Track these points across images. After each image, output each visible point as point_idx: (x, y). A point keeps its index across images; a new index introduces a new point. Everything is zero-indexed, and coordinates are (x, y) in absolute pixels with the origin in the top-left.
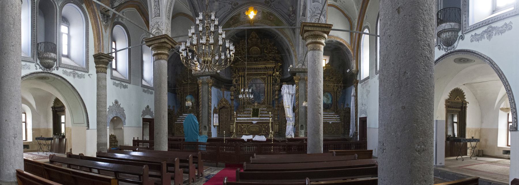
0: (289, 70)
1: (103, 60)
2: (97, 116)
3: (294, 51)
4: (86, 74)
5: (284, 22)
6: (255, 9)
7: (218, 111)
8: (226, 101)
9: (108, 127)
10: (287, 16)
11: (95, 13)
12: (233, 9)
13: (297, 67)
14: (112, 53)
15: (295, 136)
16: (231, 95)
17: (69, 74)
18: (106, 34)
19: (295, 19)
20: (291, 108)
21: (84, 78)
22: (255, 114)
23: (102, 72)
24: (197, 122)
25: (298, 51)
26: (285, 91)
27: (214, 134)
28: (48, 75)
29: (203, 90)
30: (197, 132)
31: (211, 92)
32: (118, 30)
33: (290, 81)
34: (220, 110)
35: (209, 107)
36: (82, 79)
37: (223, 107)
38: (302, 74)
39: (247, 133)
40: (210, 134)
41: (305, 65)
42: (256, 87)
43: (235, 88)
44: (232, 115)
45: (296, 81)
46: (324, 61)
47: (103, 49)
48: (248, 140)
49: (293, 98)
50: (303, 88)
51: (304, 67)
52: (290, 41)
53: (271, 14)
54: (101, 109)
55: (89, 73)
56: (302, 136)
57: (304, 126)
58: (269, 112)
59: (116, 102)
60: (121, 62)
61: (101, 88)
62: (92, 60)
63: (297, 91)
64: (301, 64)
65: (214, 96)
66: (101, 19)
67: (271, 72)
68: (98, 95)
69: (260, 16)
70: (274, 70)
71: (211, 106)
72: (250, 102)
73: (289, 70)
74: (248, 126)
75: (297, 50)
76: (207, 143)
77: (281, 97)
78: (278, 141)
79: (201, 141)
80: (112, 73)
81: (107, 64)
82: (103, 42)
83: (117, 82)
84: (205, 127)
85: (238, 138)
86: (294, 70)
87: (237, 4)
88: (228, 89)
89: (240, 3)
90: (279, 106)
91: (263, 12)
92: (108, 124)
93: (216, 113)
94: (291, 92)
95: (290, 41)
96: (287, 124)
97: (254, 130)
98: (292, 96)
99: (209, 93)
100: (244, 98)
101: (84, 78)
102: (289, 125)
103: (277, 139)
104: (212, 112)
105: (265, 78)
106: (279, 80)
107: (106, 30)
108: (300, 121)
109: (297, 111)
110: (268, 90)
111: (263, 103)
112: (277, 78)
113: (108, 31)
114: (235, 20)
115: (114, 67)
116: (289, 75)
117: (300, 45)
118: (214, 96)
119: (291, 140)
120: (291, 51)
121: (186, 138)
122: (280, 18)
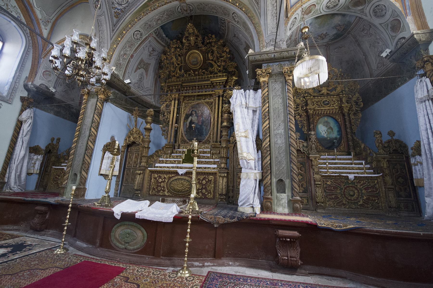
20: (252, 137)
26: (238, 102)
38: (275, 67)
49: (257, 116)
50: (279, 93)
57: (287, 182)
63: (265, 100)
86: (258, 57)
94: (251, 104)
98: (254, 111)
102: (248, 178)
108: (274, 168)
109: (265, 144)
117: (269, 13)
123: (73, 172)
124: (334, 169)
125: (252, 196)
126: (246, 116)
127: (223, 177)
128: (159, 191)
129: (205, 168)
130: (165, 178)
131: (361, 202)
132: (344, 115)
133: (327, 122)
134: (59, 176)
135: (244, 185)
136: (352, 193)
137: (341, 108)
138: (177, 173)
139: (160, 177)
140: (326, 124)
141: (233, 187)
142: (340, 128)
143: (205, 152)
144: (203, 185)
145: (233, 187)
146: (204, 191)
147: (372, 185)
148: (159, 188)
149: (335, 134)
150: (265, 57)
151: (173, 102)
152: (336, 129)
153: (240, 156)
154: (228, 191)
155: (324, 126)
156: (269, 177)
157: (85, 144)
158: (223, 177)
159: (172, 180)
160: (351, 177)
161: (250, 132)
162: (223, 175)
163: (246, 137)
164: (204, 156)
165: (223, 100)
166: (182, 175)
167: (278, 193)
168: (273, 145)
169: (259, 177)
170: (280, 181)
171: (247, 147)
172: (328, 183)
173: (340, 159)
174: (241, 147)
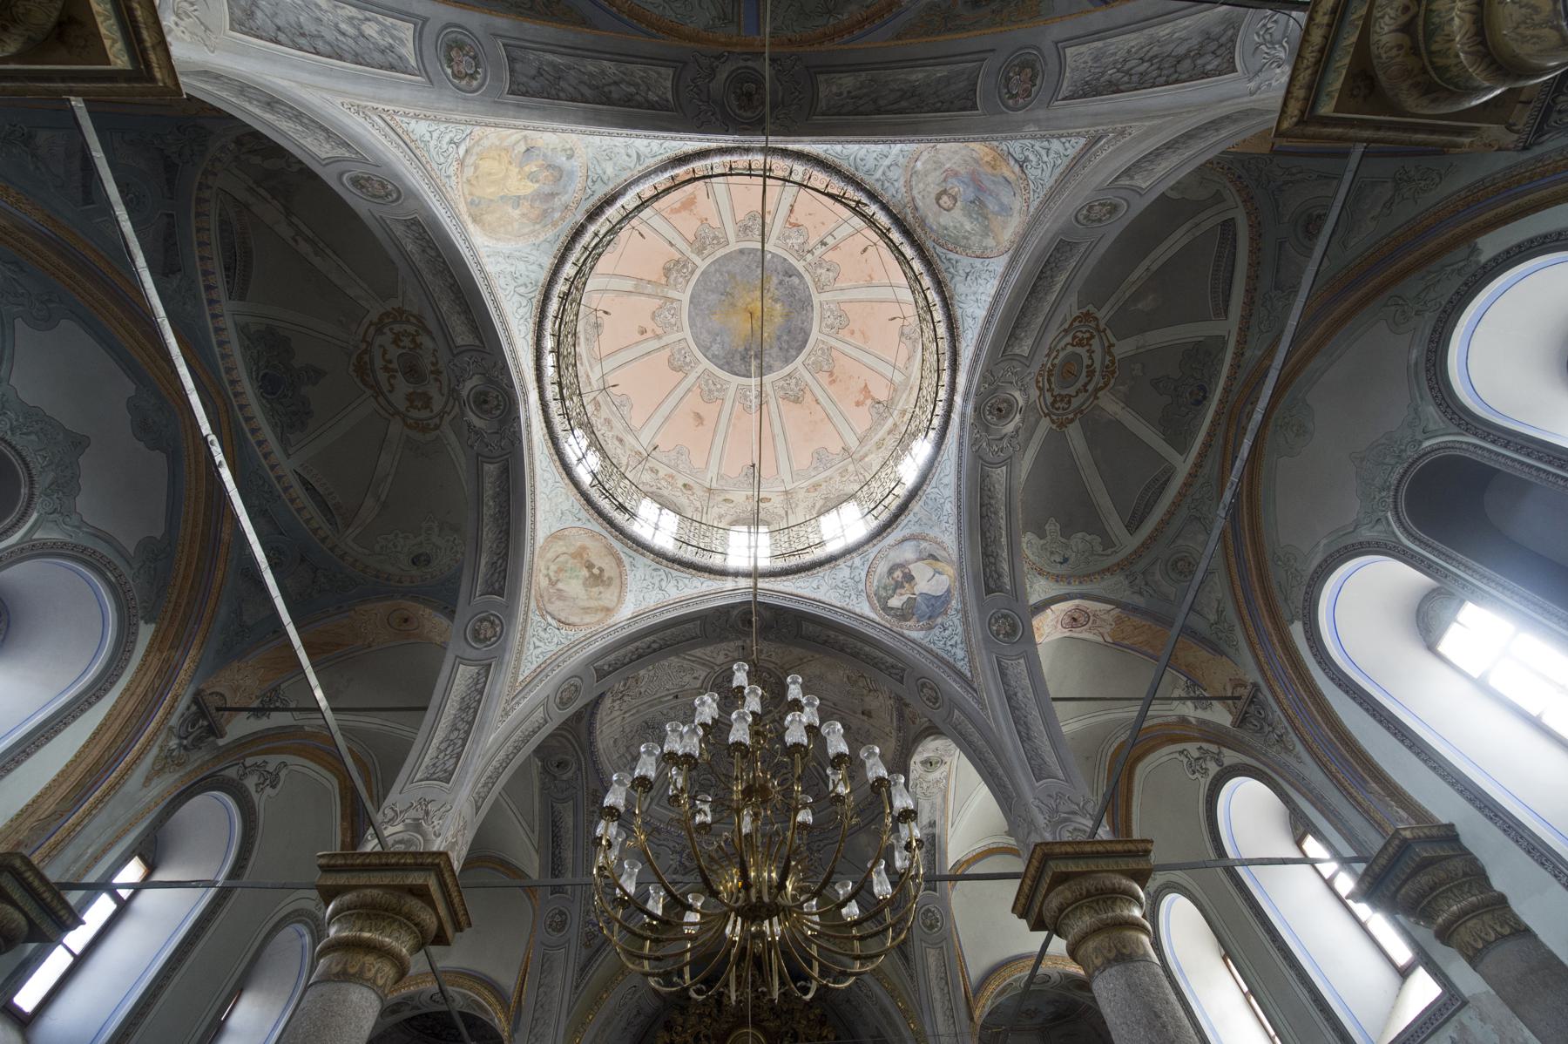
18: (141, 790)
47: (58, 848)
52: (893, 994)
66: (174, 721)
95: (893, 994)
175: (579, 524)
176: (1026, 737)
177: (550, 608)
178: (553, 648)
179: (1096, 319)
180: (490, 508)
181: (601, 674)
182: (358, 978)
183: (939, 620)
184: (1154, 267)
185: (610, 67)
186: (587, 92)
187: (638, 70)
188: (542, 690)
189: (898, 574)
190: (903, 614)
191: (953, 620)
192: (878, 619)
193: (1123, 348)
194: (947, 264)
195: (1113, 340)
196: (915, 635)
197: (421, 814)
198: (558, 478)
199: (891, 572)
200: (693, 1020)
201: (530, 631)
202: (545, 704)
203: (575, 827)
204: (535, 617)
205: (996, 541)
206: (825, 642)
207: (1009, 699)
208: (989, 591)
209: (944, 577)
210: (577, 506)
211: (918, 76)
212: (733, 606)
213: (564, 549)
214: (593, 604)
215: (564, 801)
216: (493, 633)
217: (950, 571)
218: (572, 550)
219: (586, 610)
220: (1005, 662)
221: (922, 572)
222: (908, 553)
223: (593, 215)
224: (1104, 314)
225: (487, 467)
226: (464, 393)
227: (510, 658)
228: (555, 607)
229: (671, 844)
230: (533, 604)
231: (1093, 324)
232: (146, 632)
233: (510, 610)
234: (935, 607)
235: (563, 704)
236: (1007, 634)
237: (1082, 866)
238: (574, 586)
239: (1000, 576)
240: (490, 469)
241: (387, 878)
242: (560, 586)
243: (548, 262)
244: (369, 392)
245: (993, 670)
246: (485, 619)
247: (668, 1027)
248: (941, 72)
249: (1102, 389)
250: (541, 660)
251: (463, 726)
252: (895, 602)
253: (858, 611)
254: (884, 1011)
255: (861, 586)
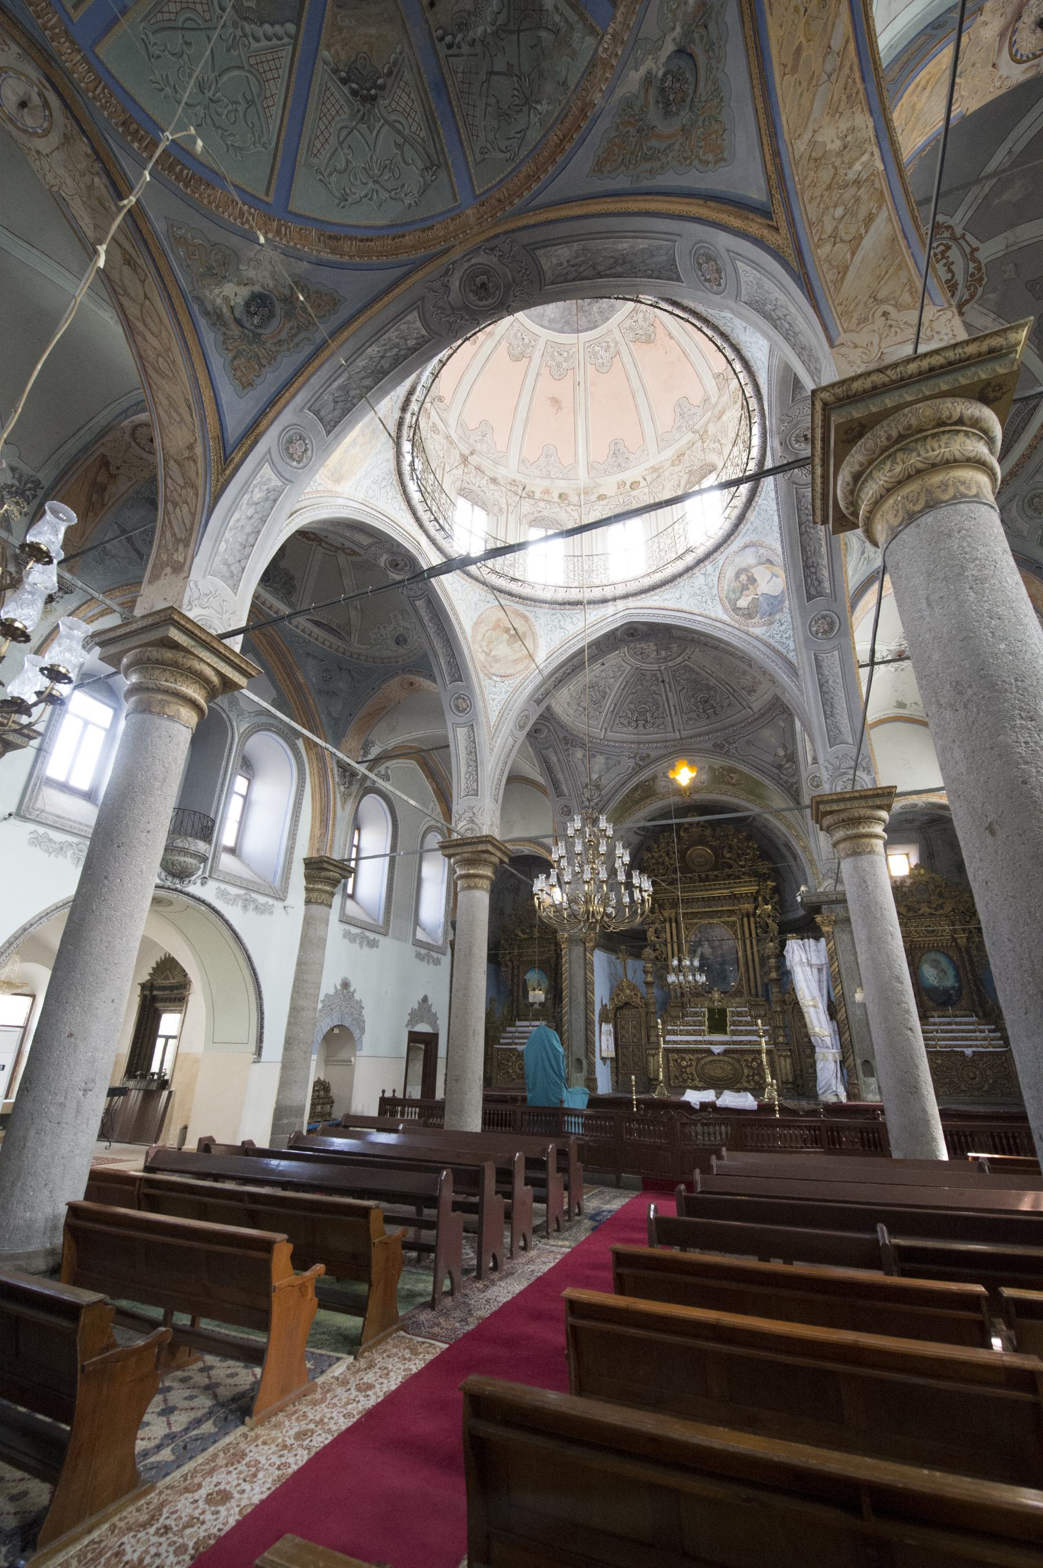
0: (799, 899)
1: (327, 874)
2: (289, 1024)
3: (805, 848)
4: (279, 905)
5: (767, 782)
6: (691, 764)
7: (611, 1015)
8: (633, 987)
9: (314, 1057)
10: (774, 770)
11: (325, 764)
12: (639, 769)
13: (822, 890)
14: (350, 860)
15: (849, 1097)
16: (646, 972)
17: (232, 901)
18: (343, 814)
19: (797, 772)
20: (822, 1007)
21: (271, 913)
22: (718, 1024)
23: (322, 903)
24: (561, 1050)
25: (818, 847)
26: (797, 959)
27: (604, 1086)
28: (174, 895)
29: (571, 959)
30: (559, 1076)
31: (592, 965)
32: (372, 803)
33: (807, 927)
34: (616, 1014)
35: (589, 1003)
36: (266, 917)
37: (627, 1004)
38: (838, 908)
39: (697, 1083)
40: (591, 1082)
41: (842, 883)
42: (713, 948)
43: (655, 950)
44: (651, 1028)
45: (825, 929)
46: (901, 863)
47: (331, 847)
48: (704, 1106)
51: (839, 888)
53: (731, 770)
54: (302, 1003)
55: (286, 903)
56: (871, 1098)
58: (756, 1017)
59: (346, 985)
60: (371, 881)
61: (311, 943)
62: (298, 871)
63: (832, 956)
64: (832, 881)
65: (600, 976)
66: (337, 779)
67: (748, 907)
68: (300, 963)
69: (704, 777)
70: (756, 899)
71: (592, 1003)
72: (699, 993)
73: (799, 899)
74: (699, 1060)
75: (812, 844)
76: (588, 1112)
77: (785, 977)
78: (794, 1112)
79: (572, 1106)
80: (343, 907)
81: (335, 883)
82: (333, 831)
83: (354, 930)
84: (579, 1061)
85: (674, 1098)
86: (814, 899)
87: (649, 756)
88: (638, 956)
89: (654, 754)
90: (784, 1002)
91: (711, 768)
92: (317, 1046)
93: (607, 1022)
94: (815, 961)
96: (818, 1056)
97: (718, 1073)
98: (820, 970)
99: (588, 966)
100: (680, 983)
101: (271, 913)
103: (790, 1104)
104: (596, 1018)
105: (734, 923)
106: (774, 927)
107: (344, 803)
108: (857, 1047)
109: (842, 1015)
110: (745, 956)
111: (738, 993)
112: (770, 921)
113: (350, 806)
114: (646, 791)
115: (350, 891)
116: (801, 912)
118: (600, 976)
119: (836, 1109)
120: (799, 850)
121: (529, 1095)
122: (757, 776)
123: (575, 1057)
124: (949, 1040)
125: (834, 1081)
126: (811, 977)
127: (785, 1057)
128: (685, 1081)
129: (750, 1042)
130: (690, 1060)
131: (986, 1088)
132: (960, 950)
133: (935, 960)
134: (508, 1061)
135: (822, 1069)
136: (972, 1075)
137: (954, 940)
138: (710, 1052)
139: (683, 1059)
140: (936, 964)
141: (801, 1071)
142: (956, 969)
143: (739, 1014)
144: (753, 1069)
145: (801, 1071)
146: (757, 1078)
147: (998, 1062)
148: (685, 1076)
149: (950, 982)
150: (824, 899)
151: (668, 924)
152: (951, 973)
153: (810, 1031)
154: (795, 1077)
155: (932, 967)
156: (852, 1058)
157: (582, 1015)
158: (785, 1057)
159: (703, 1062)
160: (968, 1052)
161: (819, 999)
162: (784, 1053)
163: (815, 1006)
164: (741, 1021)
165: (756, 923)
166: (719, 1054)
167: (865, 1076)
168: (850, 1017)
169: (838, 1058)
170: (866, 1063)
171: (819, 1020)
172: (939, 1062)
173: (960, 1024)
174: (811, 1020)
175: (489, 605)
176: (829, 713)
177: (492, 671)
178: (504, 696)
179: (949, 227)
180: (431, 629)
181: (538, 702)
182: (476, 887)
183: (777, 617)
184: (1019, 147)
185: (373, 350)
186: (367, 382)
187: (392, 334)
188: (508, 727)
189: (743, 577)
190: (748, 614)
191: (785, 616)
192: (728, 620)
193: (989, 250)
194: (724, 321)
195: (975, 243)
196: (758, 631)
197: (471, 815)
198: (463, 582)
199: (737, 576)
200: (663, 845)
201: (486, 692)
202: (512, 734)
203: (559, 760)
204: (486, 682)
205: (816, 552)
206: (692, 641)
207: (821, 686)
208: (810, 598)
209: (779, 580)
210: (483, 593)
211: (624, 245)
212: (617, 629)
213: (486, 628)
214: (518, 656)
215: (547, 748)
216: (466, 705)
217: (782, 574)
218: (492, 625)
219: (516, 661)
220: (821, 656)
221: (762, 574)
222: (749, 559)
223: (404, 409)
224: (958, 221)
225: (417, 603)
226: (382, 564)
227: (482, 718)
228: (496, 668)
229: (626, 754)
230: (482, 676)
231: (947, 234)
232: (300, 743)
233: (469, 687)
234: (774, 604)
235: (522, 728)
236: (825, 632)
237: (842, 806)
238: (503, 649)
239: (820, 582)
240: (419, 603)
241: (470, 849)
242: (493, 653)
243: (391, 454)
244: (315, 544)
245: (810, 665)
246: (457, 699)
247: (649, 849)
248: (642, 244)
249: (967, 301)
250: (499, 708)
251: (472, 763)
252: (743, 603)
253: (713, 615)
254: (784, 834)
255: (715, 591)
